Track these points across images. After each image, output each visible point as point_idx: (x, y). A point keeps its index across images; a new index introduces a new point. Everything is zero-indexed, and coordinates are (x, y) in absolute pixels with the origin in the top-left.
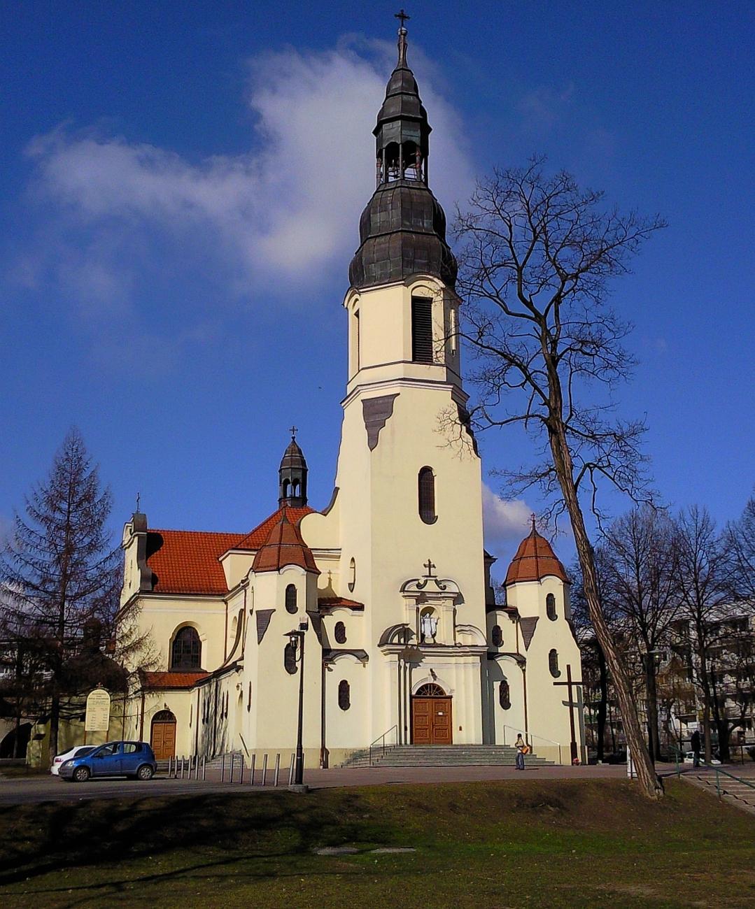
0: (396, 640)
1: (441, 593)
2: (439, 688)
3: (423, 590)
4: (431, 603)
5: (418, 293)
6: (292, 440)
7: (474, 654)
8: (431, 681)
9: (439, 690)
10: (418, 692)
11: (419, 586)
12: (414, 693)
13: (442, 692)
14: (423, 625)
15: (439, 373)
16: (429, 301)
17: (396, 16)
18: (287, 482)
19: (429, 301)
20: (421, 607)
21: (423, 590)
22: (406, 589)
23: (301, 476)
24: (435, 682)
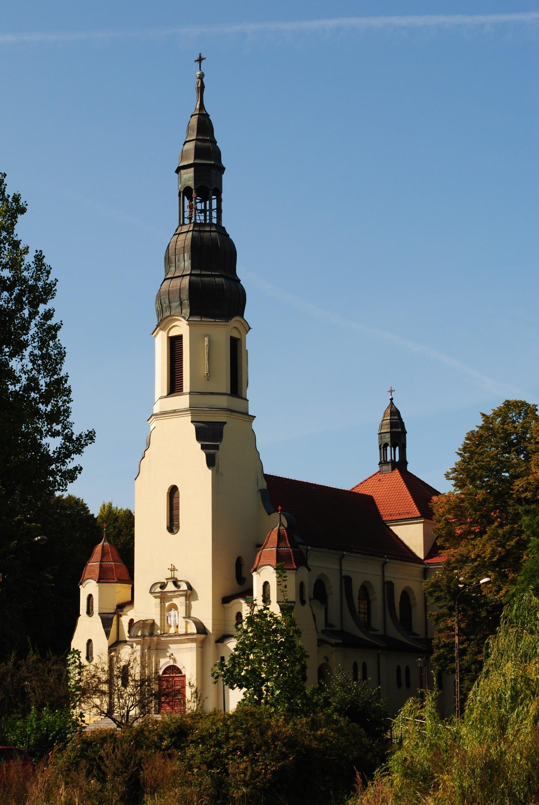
0: (139, 634)
1: (175, 591)
2: (178, 669)
3: (165, 590)
4: (175, 601)
5: (173, 333)
6: (390, 401)
7: (192, 640)
8: (171, 663)
9: (179, 671)
10: (164, 672)
11: (161, 587)
12: (161, 672)
13: (181, 672)
14: (169, 619)
15: (182, 401)
16: (179, 338)
17: (200, 55)
18: (386, 445)
19: (179, 338)
20: (167, 604)
21: (165, 590)
22: (153, 591)
23: (389, 439)
24: (175, 664)
